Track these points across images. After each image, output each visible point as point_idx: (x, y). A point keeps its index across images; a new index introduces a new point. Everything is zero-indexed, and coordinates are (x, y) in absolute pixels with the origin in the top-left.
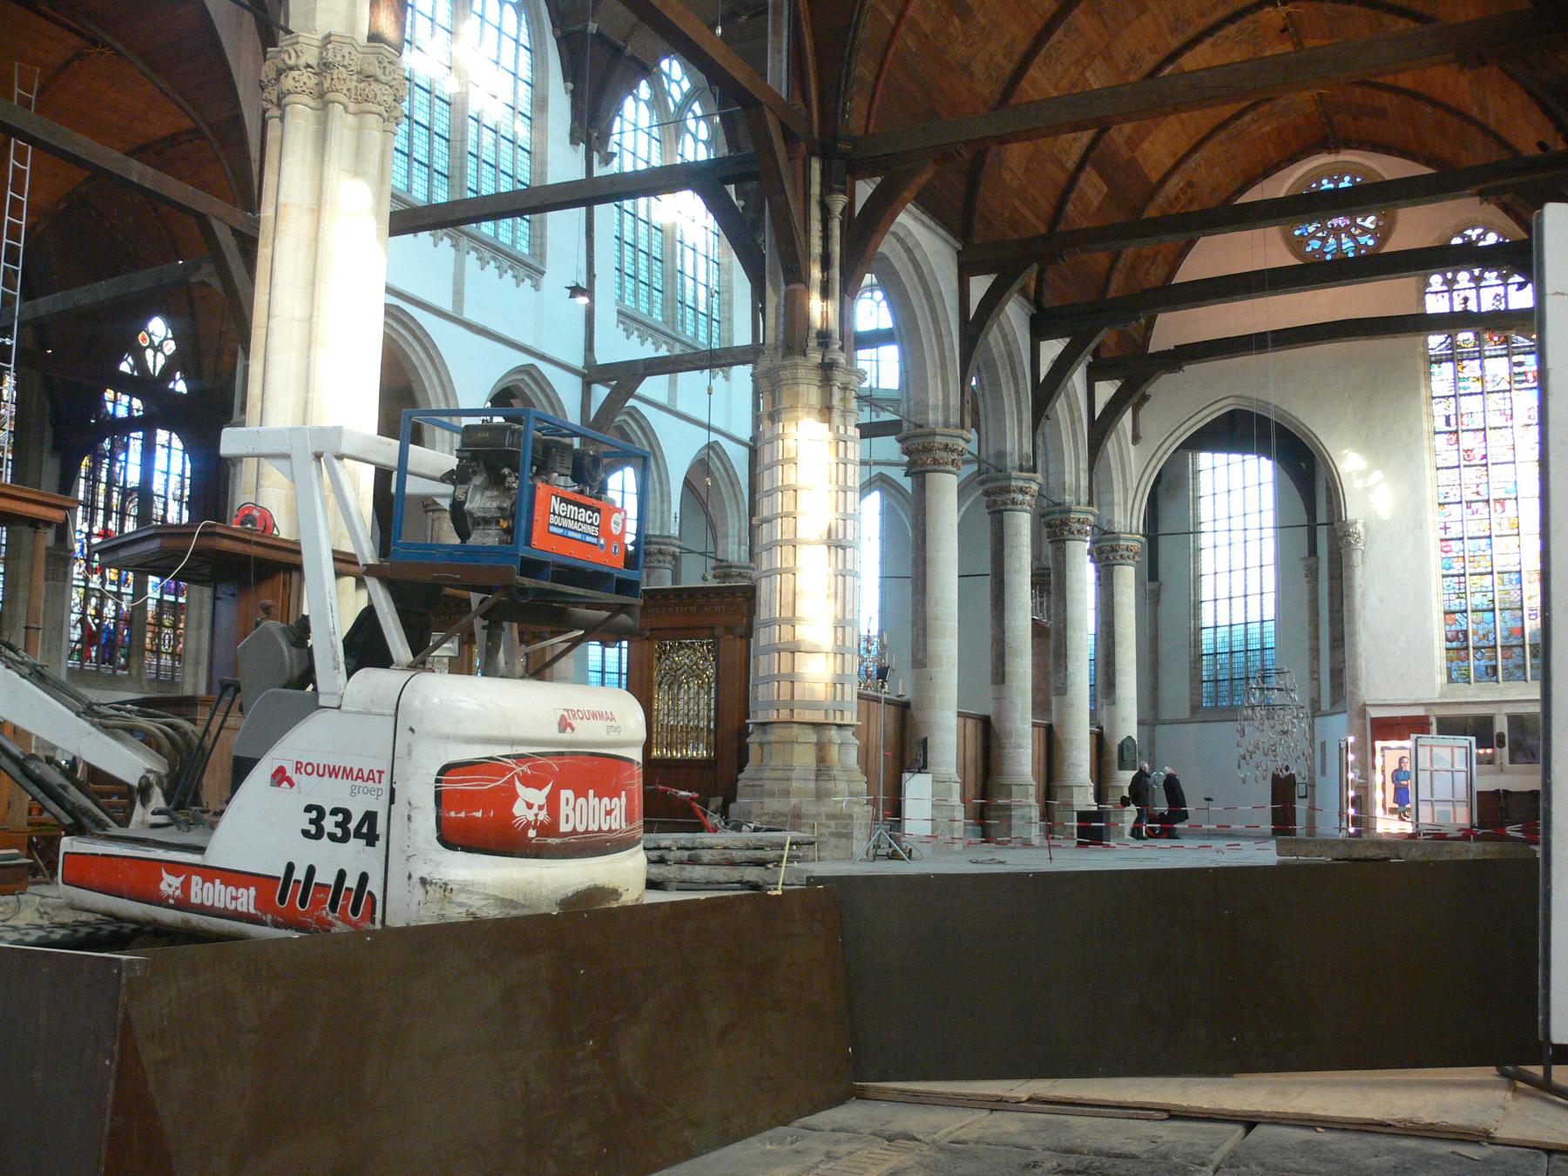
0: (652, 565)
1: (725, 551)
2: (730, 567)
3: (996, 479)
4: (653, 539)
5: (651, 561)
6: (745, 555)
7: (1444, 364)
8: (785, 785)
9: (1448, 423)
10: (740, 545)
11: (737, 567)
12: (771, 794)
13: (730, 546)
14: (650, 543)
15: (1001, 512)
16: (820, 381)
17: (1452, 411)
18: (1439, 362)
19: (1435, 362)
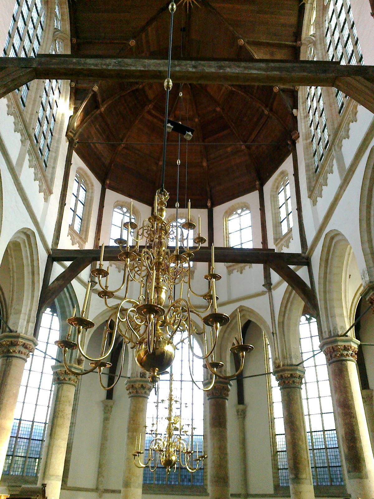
1: (16, 324)
2: (18, 337)
6: (31, 330)
10: (28, 322)
11: (23, 338)
13: (21, 321)
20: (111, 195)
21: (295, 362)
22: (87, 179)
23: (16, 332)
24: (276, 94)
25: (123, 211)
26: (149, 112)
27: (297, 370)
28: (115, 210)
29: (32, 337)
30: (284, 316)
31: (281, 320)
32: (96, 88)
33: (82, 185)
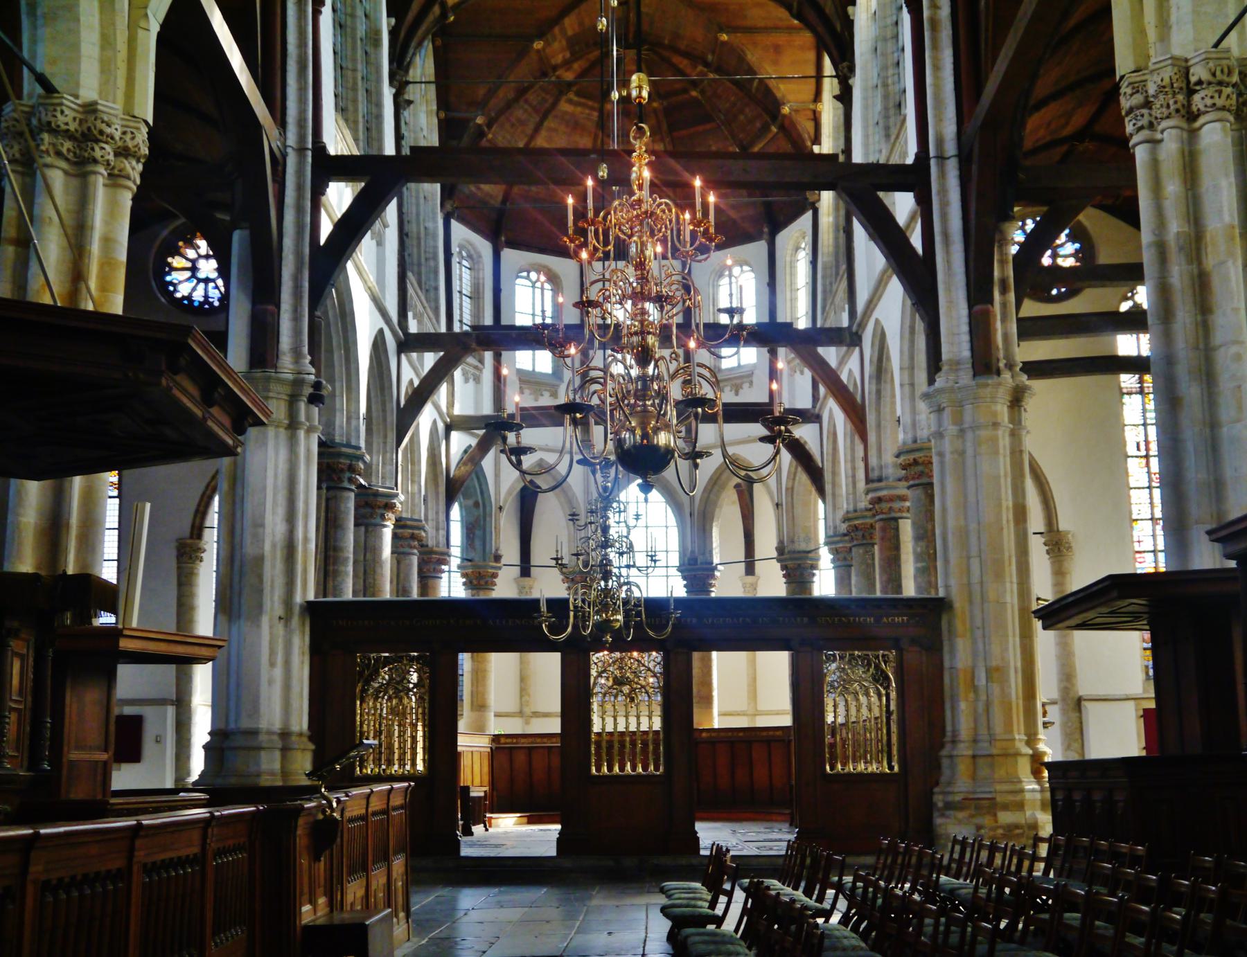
0: (402, 550)
3: (895, 488)
4: (409, 523)
5: (402, 546)
7: (1133, 396)
8: (1018, 798)
9: (1138, 449)
10: (437, 529)
11: (436, 553)
12: (1005, 807)
14: (405, 527)
15: (896, 519)
16: (1011, 402)
17: (1141, 439)
18: (1130, 394)
19: (1128, 394)
20: (508, 254)
21: (802, 546)
22: (470, 248)
23: (427, 546)
24: (785, 116)
25: (530, 281)
26: (570, 102)
27: (807, 558)
28: (519, 281)
29: (442, 548)
30: (794, 479)
31: (790, 486)
32: (479, 120)
33: (465, 263)
